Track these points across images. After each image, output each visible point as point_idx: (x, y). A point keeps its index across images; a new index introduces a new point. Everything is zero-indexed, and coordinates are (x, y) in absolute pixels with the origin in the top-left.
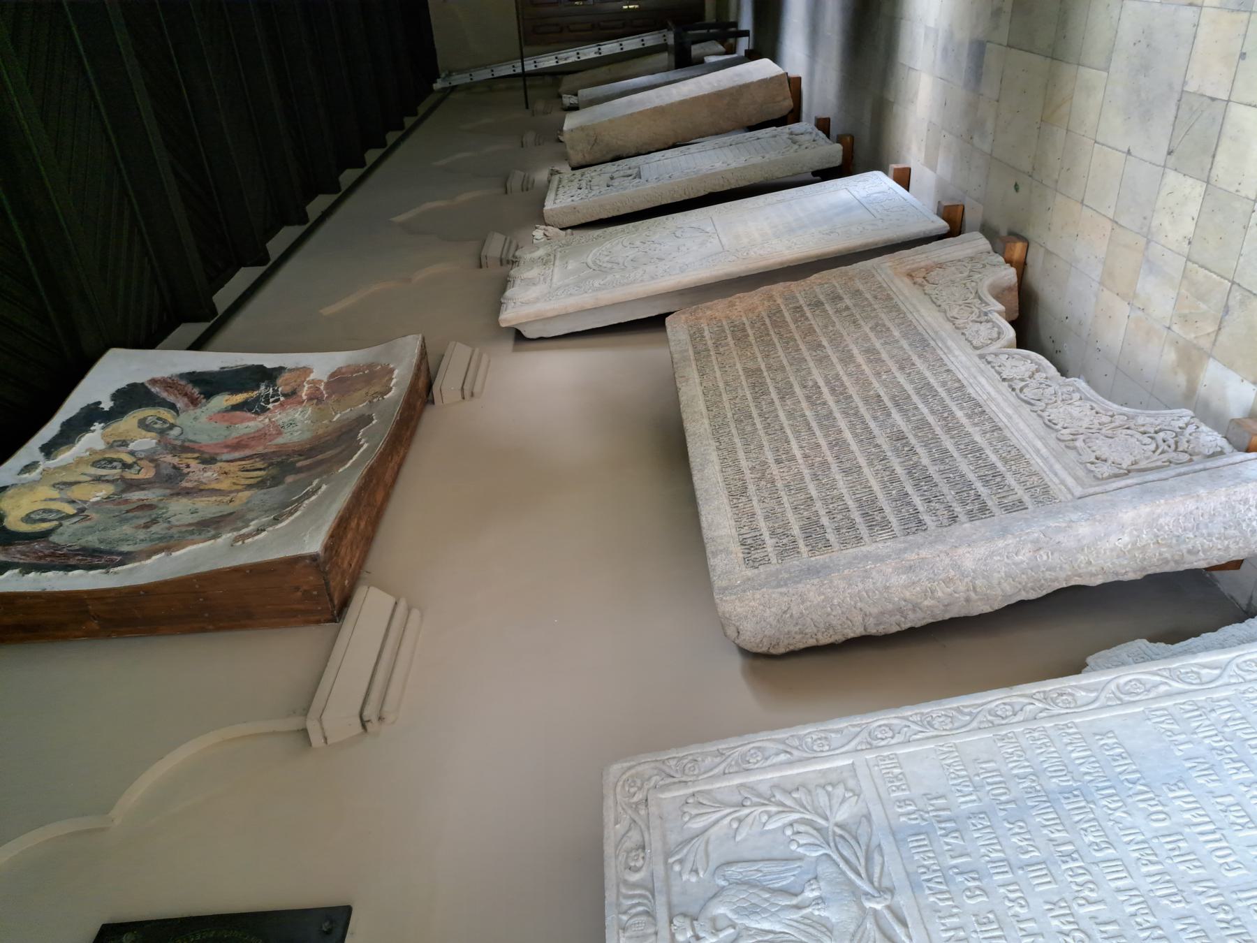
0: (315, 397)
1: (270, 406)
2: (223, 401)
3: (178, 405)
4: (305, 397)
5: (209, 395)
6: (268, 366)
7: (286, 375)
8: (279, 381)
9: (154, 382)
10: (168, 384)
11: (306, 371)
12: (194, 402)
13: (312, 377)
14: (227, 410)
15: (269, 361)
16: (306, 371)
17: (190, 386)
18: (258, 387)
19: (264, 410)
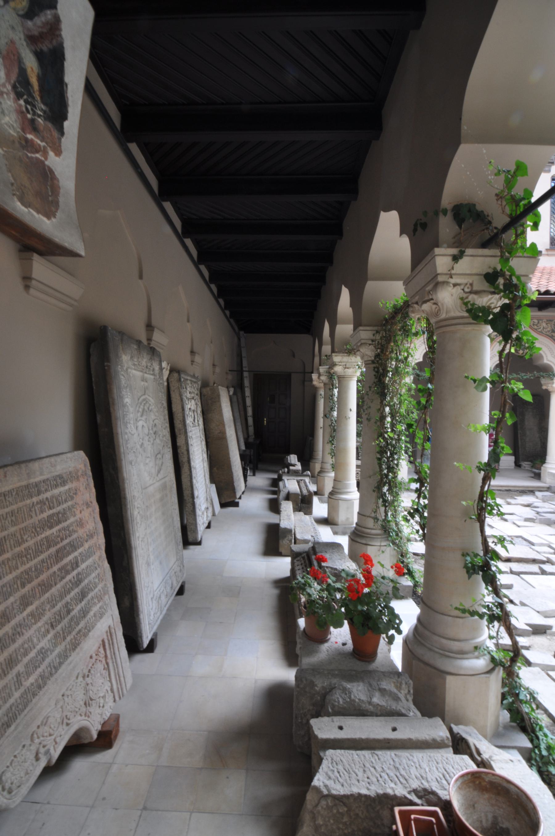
0: (28, 145)
1: (22, 102)
2: (31, 63)
3: (29, 23)
4: (30, 136)
5: (39, 56)
6: (66, 124)
7: (56, 134)
8: (50, 125)
9: (57, 20)
10: (54, 26)
11: (58, 152)
12: (32, 39)
13: (51, 154)
14: (20, 61)
15: (72, 124)
16: (58, 152)
17: (50, 46)
18: (45, 104)
19: (19, 96)
